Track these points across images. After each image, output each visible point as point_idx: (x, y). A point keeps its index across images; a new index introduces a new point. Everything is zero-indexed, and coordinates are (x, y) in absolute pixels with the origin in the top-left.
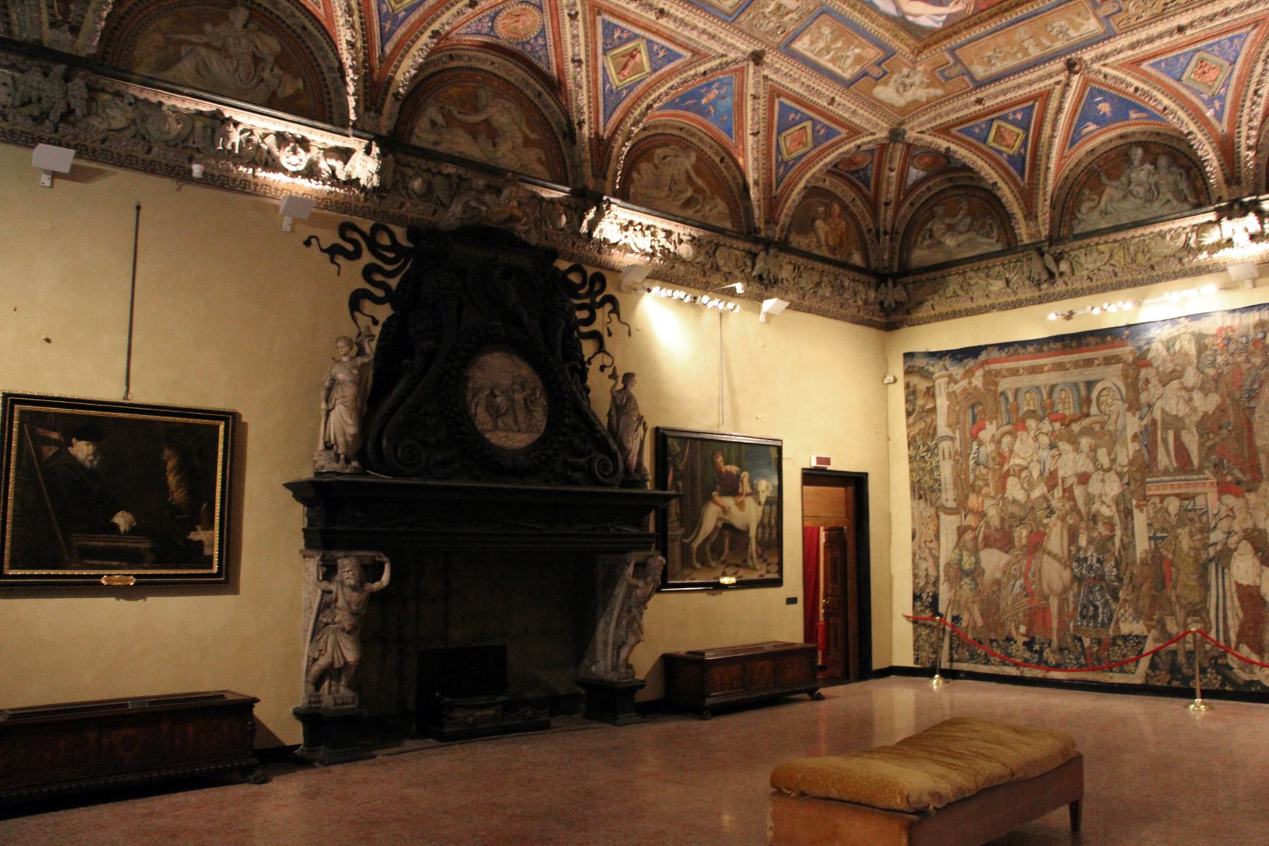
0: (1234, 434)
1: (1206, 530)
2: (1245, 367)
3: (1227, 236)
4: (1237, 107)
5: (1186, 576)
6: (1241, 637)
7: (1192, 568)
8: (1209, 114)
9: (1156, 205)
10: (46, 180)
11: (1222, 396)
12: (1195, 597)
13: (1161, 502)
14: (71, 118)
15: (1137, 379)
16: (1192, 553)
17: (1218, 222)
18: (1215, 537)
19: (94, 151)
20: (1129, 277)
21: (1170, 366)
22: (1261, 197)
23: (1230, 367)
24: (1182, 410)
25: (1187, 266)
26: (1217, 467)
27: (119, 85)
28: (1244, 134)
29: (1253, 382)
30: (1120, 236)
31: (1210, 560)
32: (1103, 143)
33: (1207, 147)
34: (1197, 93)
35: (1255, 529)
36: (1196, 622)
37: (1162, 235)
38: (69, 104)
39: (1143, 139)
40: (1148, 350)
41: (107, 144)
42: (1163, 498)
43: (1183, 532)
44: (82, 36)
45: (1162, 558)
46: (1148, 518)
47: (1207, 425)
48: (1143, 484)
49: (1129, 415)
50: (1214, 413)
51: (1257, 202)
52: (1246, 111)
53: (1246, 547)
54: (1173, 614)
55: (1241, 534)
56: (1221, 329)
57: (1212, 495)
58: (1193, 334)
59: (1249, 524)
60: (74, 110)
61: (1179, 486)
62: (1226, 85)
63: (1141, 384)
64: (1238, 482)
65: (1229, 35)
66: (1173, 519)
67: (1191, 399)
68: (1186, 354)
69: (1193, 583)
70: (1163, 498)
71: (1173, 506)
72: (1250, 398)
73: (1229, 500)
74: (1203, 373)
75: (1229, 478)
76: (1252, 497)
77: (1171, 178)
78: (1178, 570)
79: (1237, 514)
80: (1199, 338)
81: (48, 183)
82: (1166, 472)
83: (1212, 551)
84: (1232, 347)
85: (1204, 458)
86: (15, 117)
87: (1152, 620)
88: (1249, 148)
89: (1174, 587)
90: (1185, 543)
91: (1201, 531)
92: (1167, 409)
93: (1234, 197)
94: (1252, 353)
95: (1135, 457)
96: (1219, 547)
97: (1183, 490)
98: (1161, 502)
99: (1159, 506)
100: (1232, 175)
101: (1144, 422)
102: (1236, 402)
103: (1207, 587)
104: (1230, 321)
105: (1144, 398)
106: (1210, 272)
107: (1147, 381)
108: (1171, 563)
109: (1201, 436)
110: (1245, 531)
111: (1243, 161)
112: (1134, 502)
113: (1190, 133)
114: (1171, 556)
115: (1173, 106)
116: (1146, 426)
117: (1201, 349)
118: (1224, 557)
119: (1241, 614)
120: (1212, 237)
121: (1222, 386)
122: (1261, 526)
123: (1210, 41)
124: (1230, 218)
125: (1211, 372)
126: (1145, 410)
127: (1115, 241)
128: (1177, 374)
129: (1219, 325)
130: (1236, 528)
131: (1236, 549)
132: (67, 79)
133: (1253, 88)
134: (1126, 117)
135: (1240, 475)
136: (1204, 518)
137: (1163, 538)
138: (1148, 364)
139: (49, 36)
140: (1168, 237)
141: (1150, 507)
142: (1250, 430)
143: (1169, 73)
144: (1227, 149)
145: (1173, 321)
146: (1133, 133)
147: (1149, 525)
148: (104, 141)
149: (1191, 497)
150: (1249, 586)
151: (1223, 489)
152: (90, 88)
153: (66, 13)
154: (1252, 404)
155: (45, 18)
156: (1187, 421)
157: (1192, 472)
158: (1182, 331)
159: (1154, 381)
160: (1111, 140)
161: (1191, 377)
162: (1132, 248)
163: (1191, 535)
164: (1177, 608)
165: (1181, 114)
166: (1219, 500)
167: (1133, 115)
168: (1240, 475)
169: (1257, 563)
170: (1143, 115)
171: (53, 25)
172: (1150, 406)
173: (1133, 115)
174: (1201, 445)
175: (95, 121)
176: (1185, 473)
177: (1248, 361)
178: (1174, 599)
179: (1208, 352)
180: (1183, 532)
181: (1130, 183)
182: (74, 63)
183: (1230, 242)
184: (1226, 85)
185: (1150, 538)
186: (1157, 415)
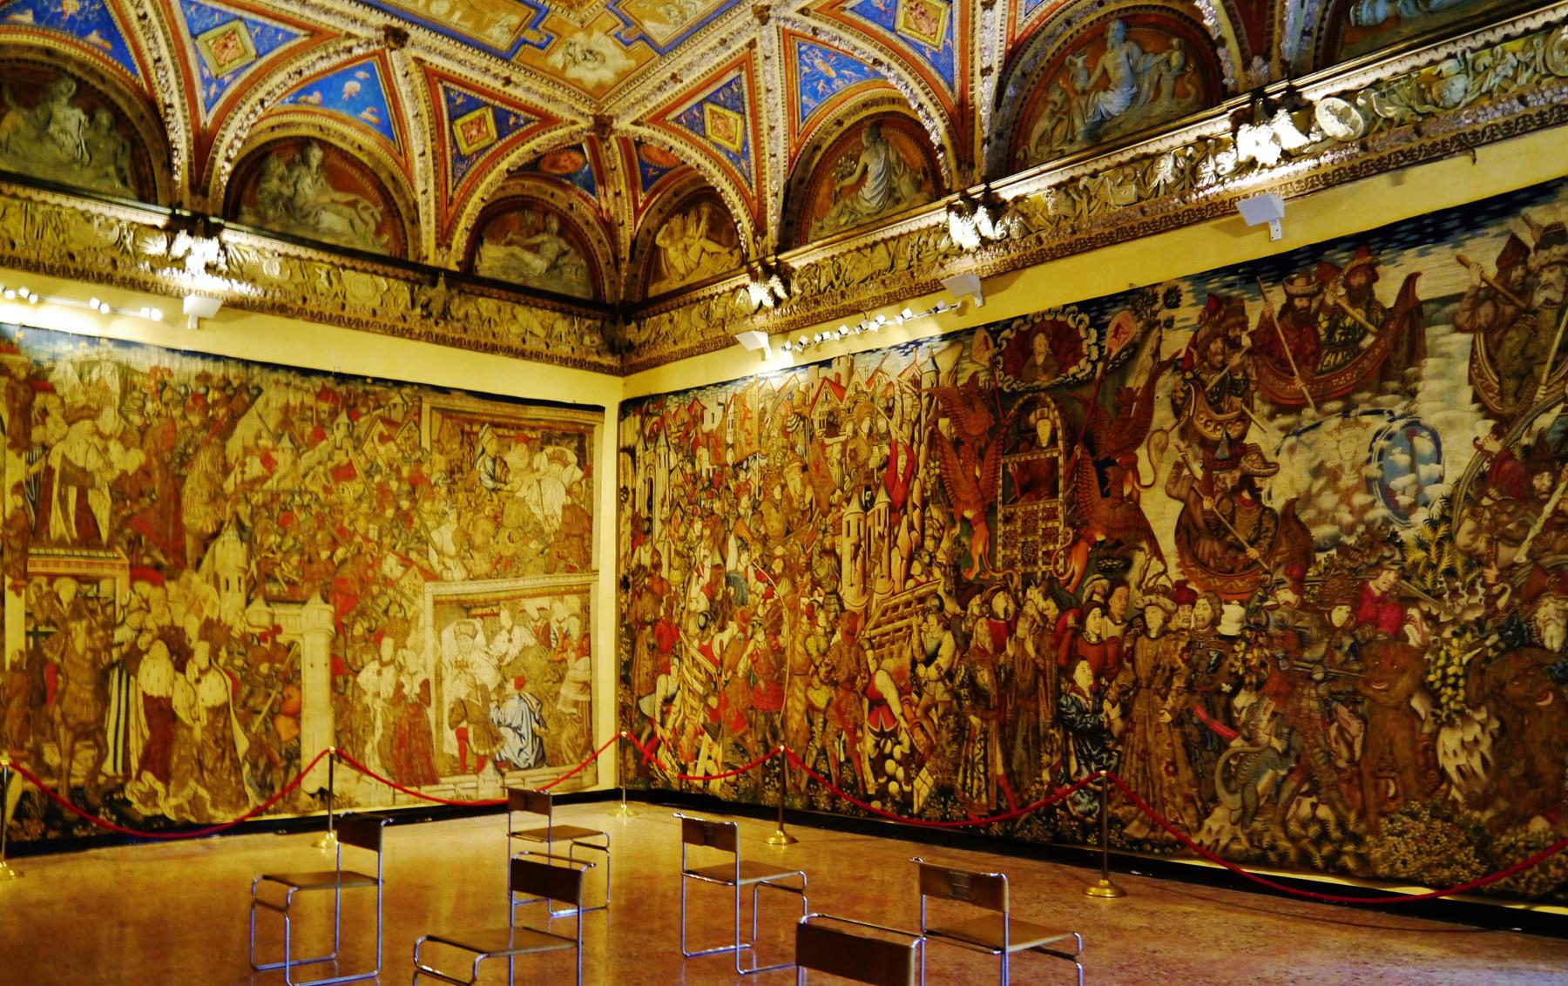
0: (158, 506)
1: (111, 625)
2: (180, 424)
3: (178, 249)
4: (233, 104)
5: (77, 690)
6: (145, 763)
7: (86, 676)
8: (200, 95)
9: (89, 173)
11: (148, 454)
12: (88, 714)
13: (50, 584)
15: (28, 406)
16: (89, 655)
17: (171, 230)
18: (122, 634)
20: (34, 255)
21: (81, 400)
22: (228, 224)
23: (163, 420)
24: (93, 462)
25: (121, 272)
26: (133, 545)
28: (227, 141)
29: (187, 445)
30: (29, 192)
31: (112, 665)
32: (17, 46)
33: (182, 133)
34: (202, 64)
35: (172, 627)
36: (88, 747)
37: (88, 218)
39: (78, 73)
40: (51, 369)
42: (52, 578)
43: (79, 628)
45: (45, 661)
46: (27, 604)
47: (122, 490)
48: (25, 554)
49: (11, 455)
50: (136, 474)
51: (220, 228)
52: (241, 115)
53: (160, 649)
54: (55, 739)
55: (156, 632)
56: (155, 369)
57: (123, 578)
58: (119, 364)
59: (166, 621)
61: (79, 565)
62: (236, 74)
63: (34, 414)
64: (158, 567)
65: (282, 26)
66: (66, 610)
67: (106, 449)
68: (106, 389)
69: (88, 696)
70: (52, 578)
71: (67, 590)
72: (182, 464)
73: (144, 588)
74: (126, 419)
75: (147, 561)
76: (171, 586)
77: (112, 146)
78: (67, 678)
79: (153, 607)
80: (126, 373)
82: (61, 543)
83: (115, 653)
84: (167, 395)
85: (116, 532)
87: (22, 748)
88: (228, 159)
89: (60, 702)
90: (80, 642)
91: (104, 626)
92: (71, 456)
93: (199, 209)
94: (191, 410)
95: (14, 517)
96: (125, 649)
97: (84, 570)
98: (50, 584)
99: (45, 588)
100: (199, 184)
101: (34, 469)
102: (165, 466)
103: (106, 701)
104: (166, 361)
105: (37, 434)
106: (147, 290)
107: (45, 413)
108: (58, 669)
109: (114, 501)
110: (161, 629)
111: (216, 169)
112: (8, 581)
113: (171, 106)
114: (57, 659)
115: (167, 61)
116: (36, 476)
117: (127, 387)
118: (131, 661)
119: (147, 733)
120: (156, 246)
121: (149, 441)
122: (179, 623)
123: (260, 19)
124: (191, 234)
125: (137, 420)
126: (37, 451)
127: (15, 196)
128: (90, 413)
129: (154, 363)
130: (150, 624)
131: (147, 651)
133: (261, 94)
134: (83, 33)
135: (161, 559)
136: (109, 610)
137: (47, 635)
138: (50, 389)
140: (96, 223)
141: (32, 589)
142: (178, 502)
143: (190, 22)
144: (203, 145)
145: (92, 340)
146: (68, 58)
147: (29, 615)
149: (95, 581)
150: (160, 698)
151: (137, 573)
154: (184, 472)
156: (98, 478)
157: (99, 547)
158: (105, 356)
159: (55, 414)
160: (30, 48)
161: (109, 421)
162: (38, 218)
163: (90, 631)
164: (62, 731)
165: (172, 75)
166: (132, 588)
167: (94, 37)
168: (161, 559)
169: (170, 667)
170: (108, 46)
172: (46, 448)
173: (94, 37)
174: (114, 513)
176: (88, 547)
177: (184, 417)
178: (58, 718)
179: (136, 394)
180: (79, 628)
181: (48, 123)
183: (179, 263)
184: (236, 74)
185: (28, 634)
186: (56, 462)
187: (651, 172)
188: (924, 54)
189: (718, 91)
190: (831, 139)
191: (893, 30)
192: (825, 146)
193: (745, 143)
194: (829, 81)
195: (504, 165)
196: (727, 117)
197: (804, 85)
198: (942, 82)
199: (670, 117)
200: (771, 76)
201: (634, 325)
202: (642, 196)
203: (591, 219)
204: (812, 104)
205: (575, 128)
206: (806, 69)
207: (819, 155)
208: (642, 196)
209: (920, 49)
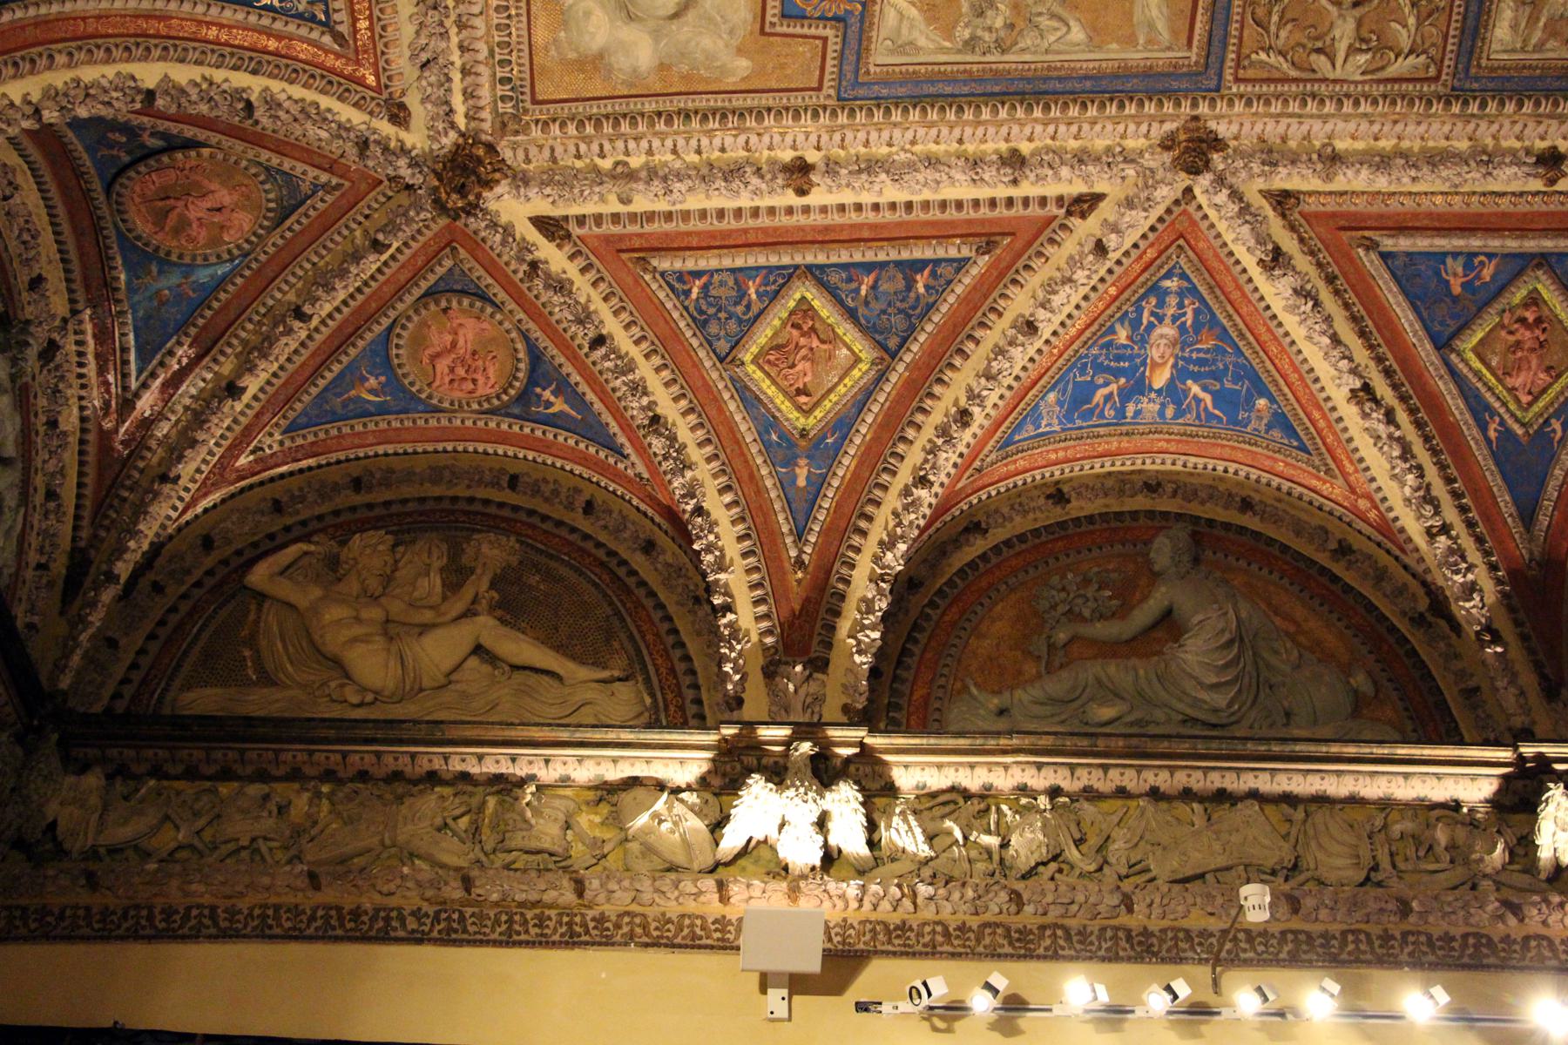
187: (369, 390)
188: (1483, 428)
189: (869, 267)
190: (1020, 524)
191: (1443, 344)
192: (998, 535)
193: (843, 425)
194: (1139, 387)
195: (149, 74)
196: (833, 339)
197: (1096, 366)
198: (1505, 501)
199: (664, 264)
200: (1057, 298)
201: (93, 780)
202: (271, 441)
203: (70, 420)
204: (1050, 422)
205: (385, 128)
206: (1122, 335)
207: (979, 546)
208: (271, 441)
209: (1479, 410)
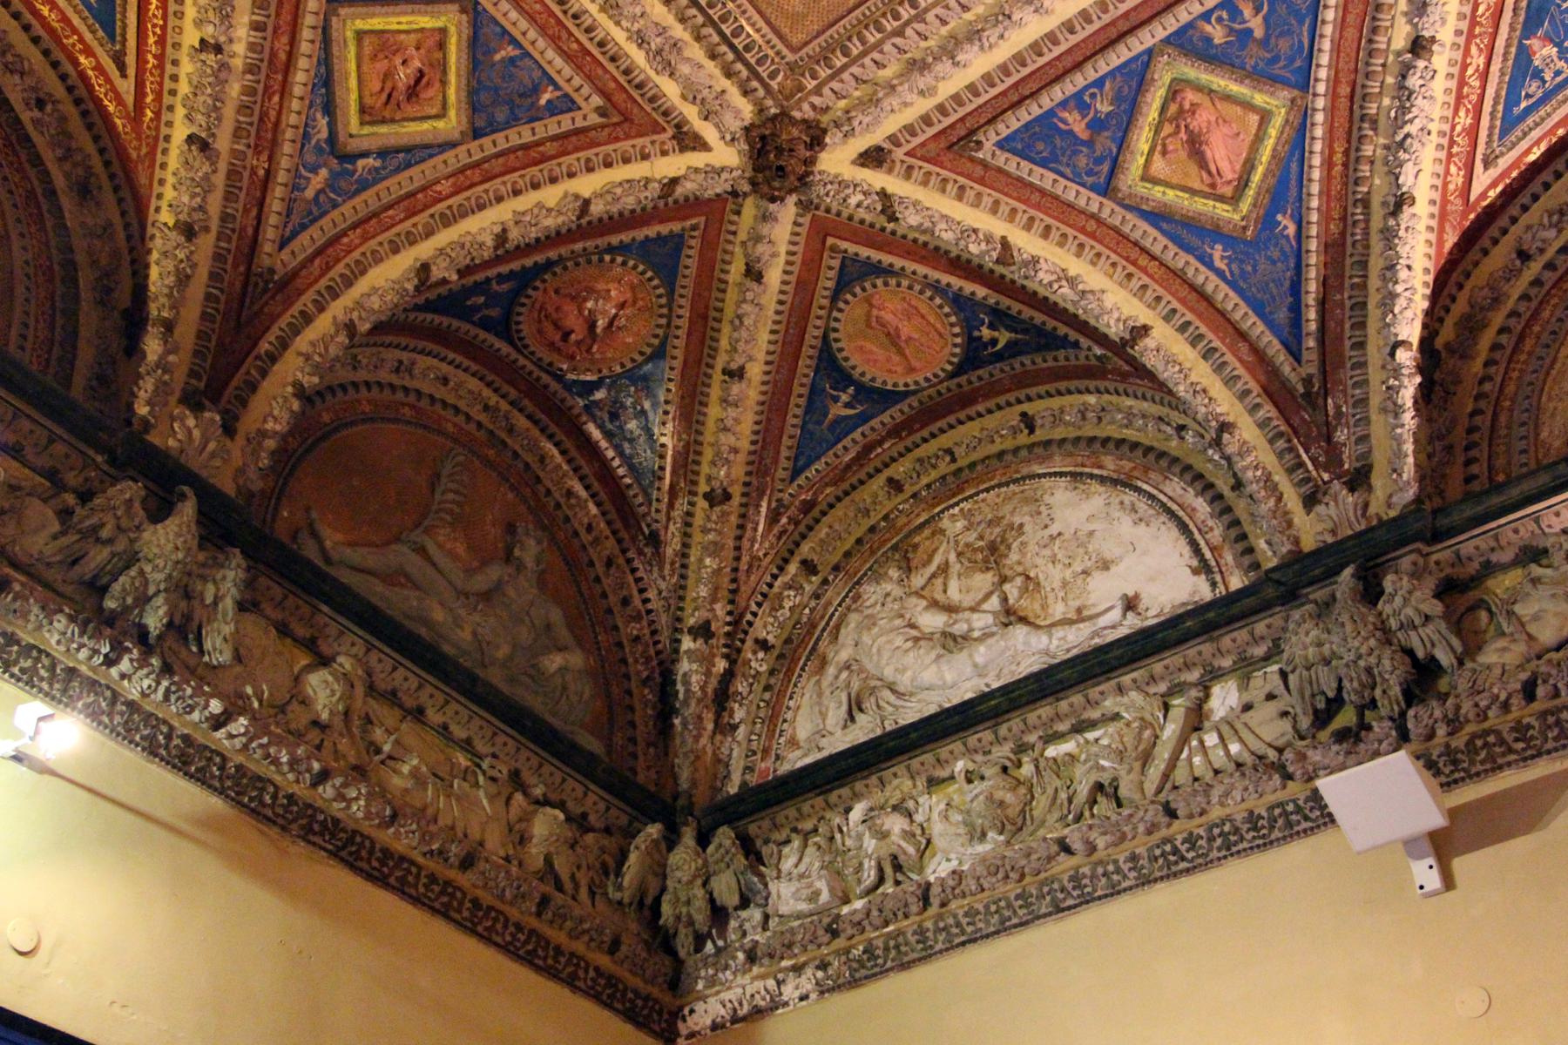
10: (1425, 873)
14: (1443, 684)
19: (1521, 729)
27: (1515, 528)
38: (1409, 652)
41: (1541, 691)
44: (1377, 481)
60: (1433, 659)
81: (1433, 880)
86: (1302, 757)
132: (1371, 593)
139: (1311, 530)
148: (1529, 691)
152: (1448, 589)
153: (1332, 459)
155: (1292, 501)
171: (1310, 501)
175: (1490, 656)
182: (1367, 556)
